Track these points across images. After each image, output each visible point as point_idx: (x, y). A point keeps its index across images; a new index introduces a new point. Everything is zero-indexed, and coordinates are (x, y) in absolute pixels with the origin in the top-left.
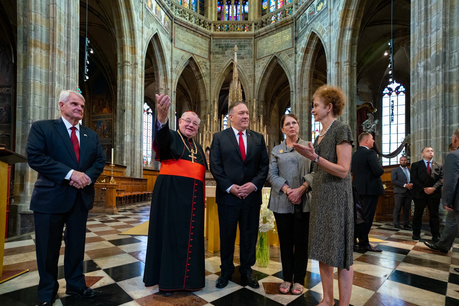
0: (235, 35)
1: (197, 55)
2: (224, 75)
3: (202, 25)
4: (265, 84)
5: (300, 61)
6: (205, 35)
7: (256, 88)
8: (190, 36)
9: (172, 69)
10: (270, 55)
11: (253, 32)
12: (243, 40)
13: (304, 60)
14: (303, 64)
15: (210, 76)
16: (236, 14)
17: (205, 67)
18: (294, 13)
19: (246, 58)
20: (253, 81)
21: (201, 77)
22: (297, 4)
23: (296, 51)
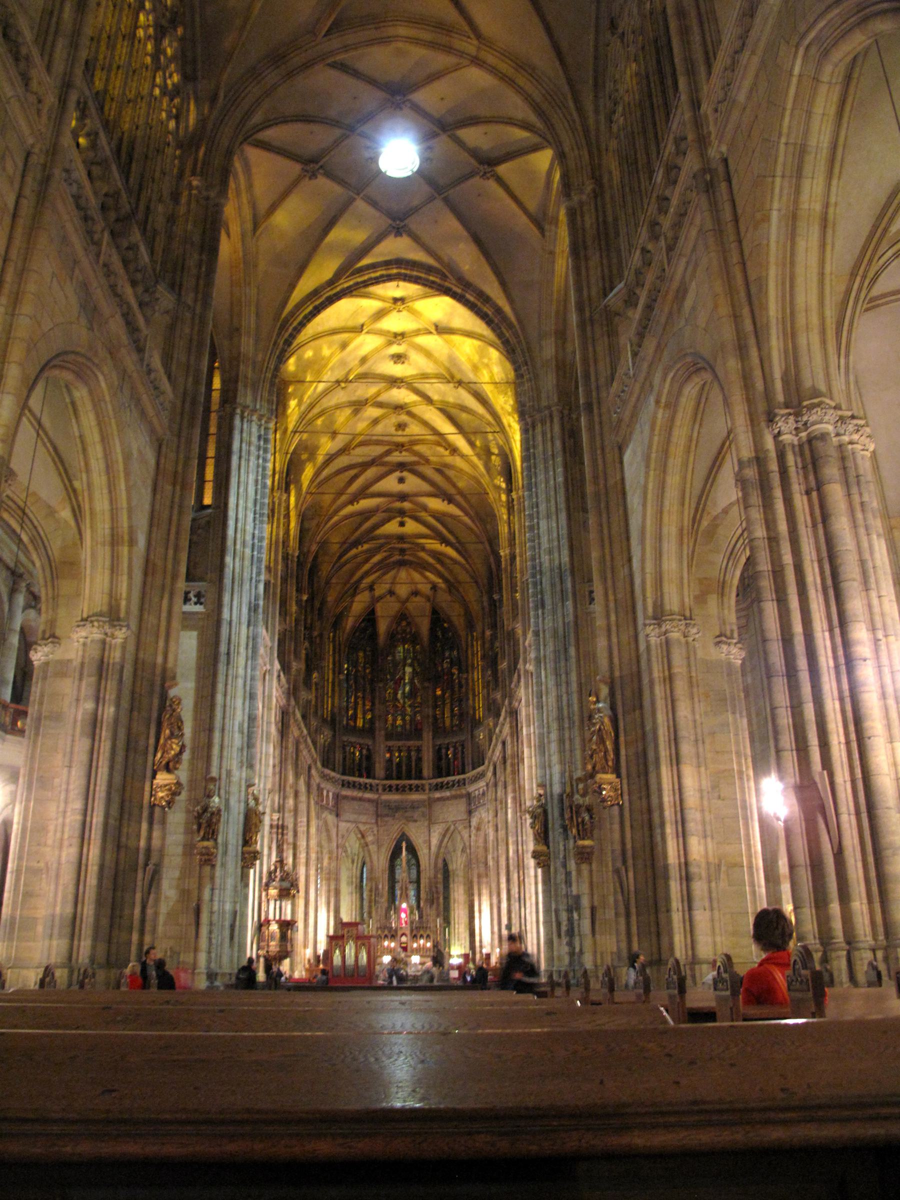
8: (356, 804)
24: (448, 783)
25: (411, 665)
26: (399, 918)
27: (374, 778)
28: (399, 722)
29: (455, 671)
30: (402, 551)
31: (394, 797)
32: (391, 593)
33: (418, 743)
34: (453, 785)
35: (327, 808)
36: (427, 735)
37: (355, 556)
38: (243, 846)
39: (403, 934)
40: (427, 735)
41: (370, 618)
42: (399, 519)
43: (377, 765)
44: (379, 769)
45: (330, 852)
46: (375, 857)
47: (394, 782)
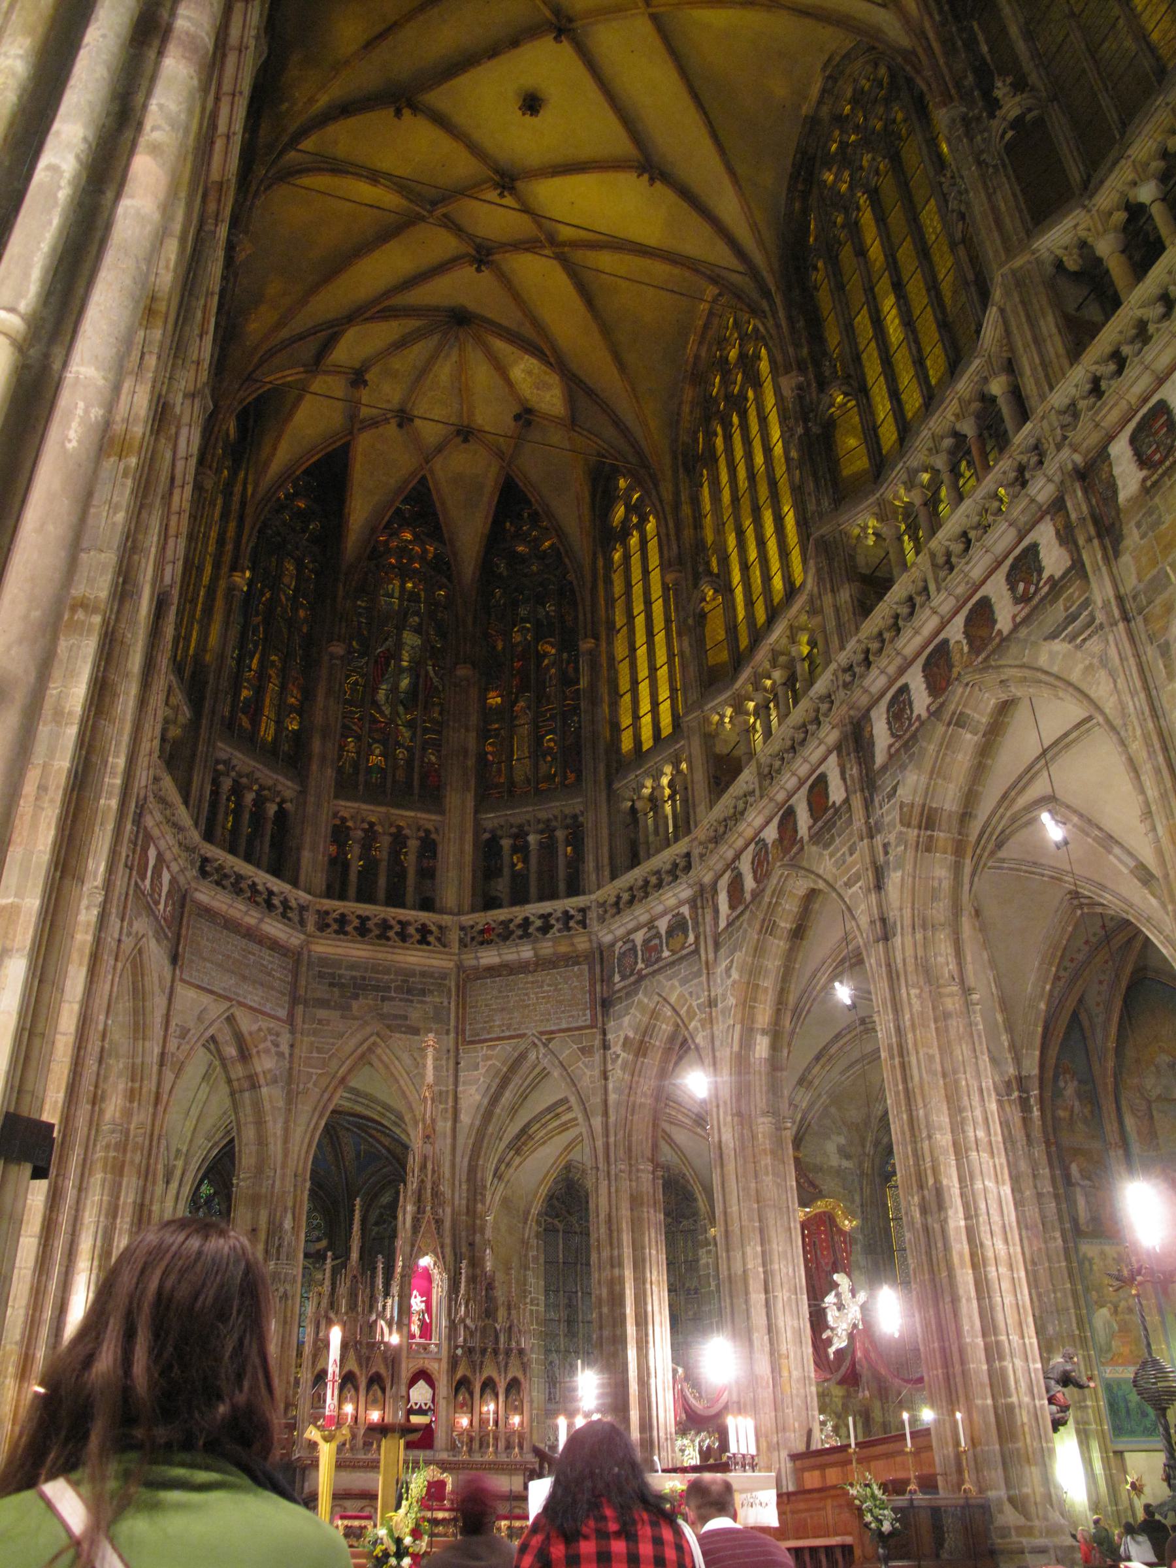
7: (461, 1140)
9: (163, 1054)
17: (273, 1050)
20: (449, 1115)
23: (604, 1040)
24: (526, 922)
25: (418, 630)
26: (405, 1309)
27: (295, 883)
28: (375, 759)
30: (483, 255)
31: (356, 951)
32: (404, 418)
33: (429, 819)
34: (545, 929)
35: (151, 912)
36: (459, 802)
39: (422, 1375)
40: (459, 802)
41: (329, 474)
43: (306, 855)
44: (313, 857)
45: (135, 1074)
46: (275, 1127)
47: (353, 908)
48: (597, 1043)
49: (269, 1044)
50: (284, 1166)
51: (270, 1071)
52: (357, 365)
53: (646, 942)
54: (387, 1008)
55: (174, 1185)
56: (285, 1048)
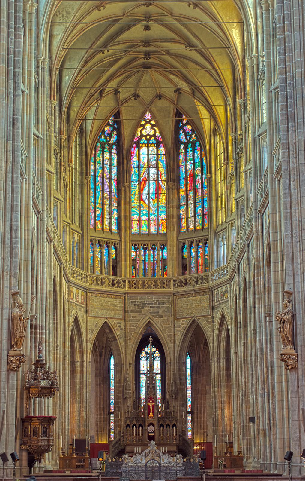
0: (152, 294)
1: (111, 318)
2: (141, 333)
3: (117, 285)
4: (186, 344)
5: (216, 332)
6: (119, 294)
7: (176, 349)
9: (87, 340)
10: (190, 317)
11: (171, 289)
12: (161, 297)
13: (219, 332)
14: (219, 336)
15: (125, 337)
16: (154, 260)
18: (211, 284)
19: (166, 316)
20: (173, 341)
21: (115, 339)
22: (212, 275)
23: (213, 320)
29: (198, 171)
30: (147, 55)
32: (136, 96)
34: (197, 282)
37: (102, 60)
38: (8, 350)
42: (144, 23)
48: (211, 321)
49: (118, 327)
50: (126, 362)
51: (119, 335)
52: (115, 86)
53: (221, 292)
54: (152, 310)
55: (103, 357)
56: (123, 327)
